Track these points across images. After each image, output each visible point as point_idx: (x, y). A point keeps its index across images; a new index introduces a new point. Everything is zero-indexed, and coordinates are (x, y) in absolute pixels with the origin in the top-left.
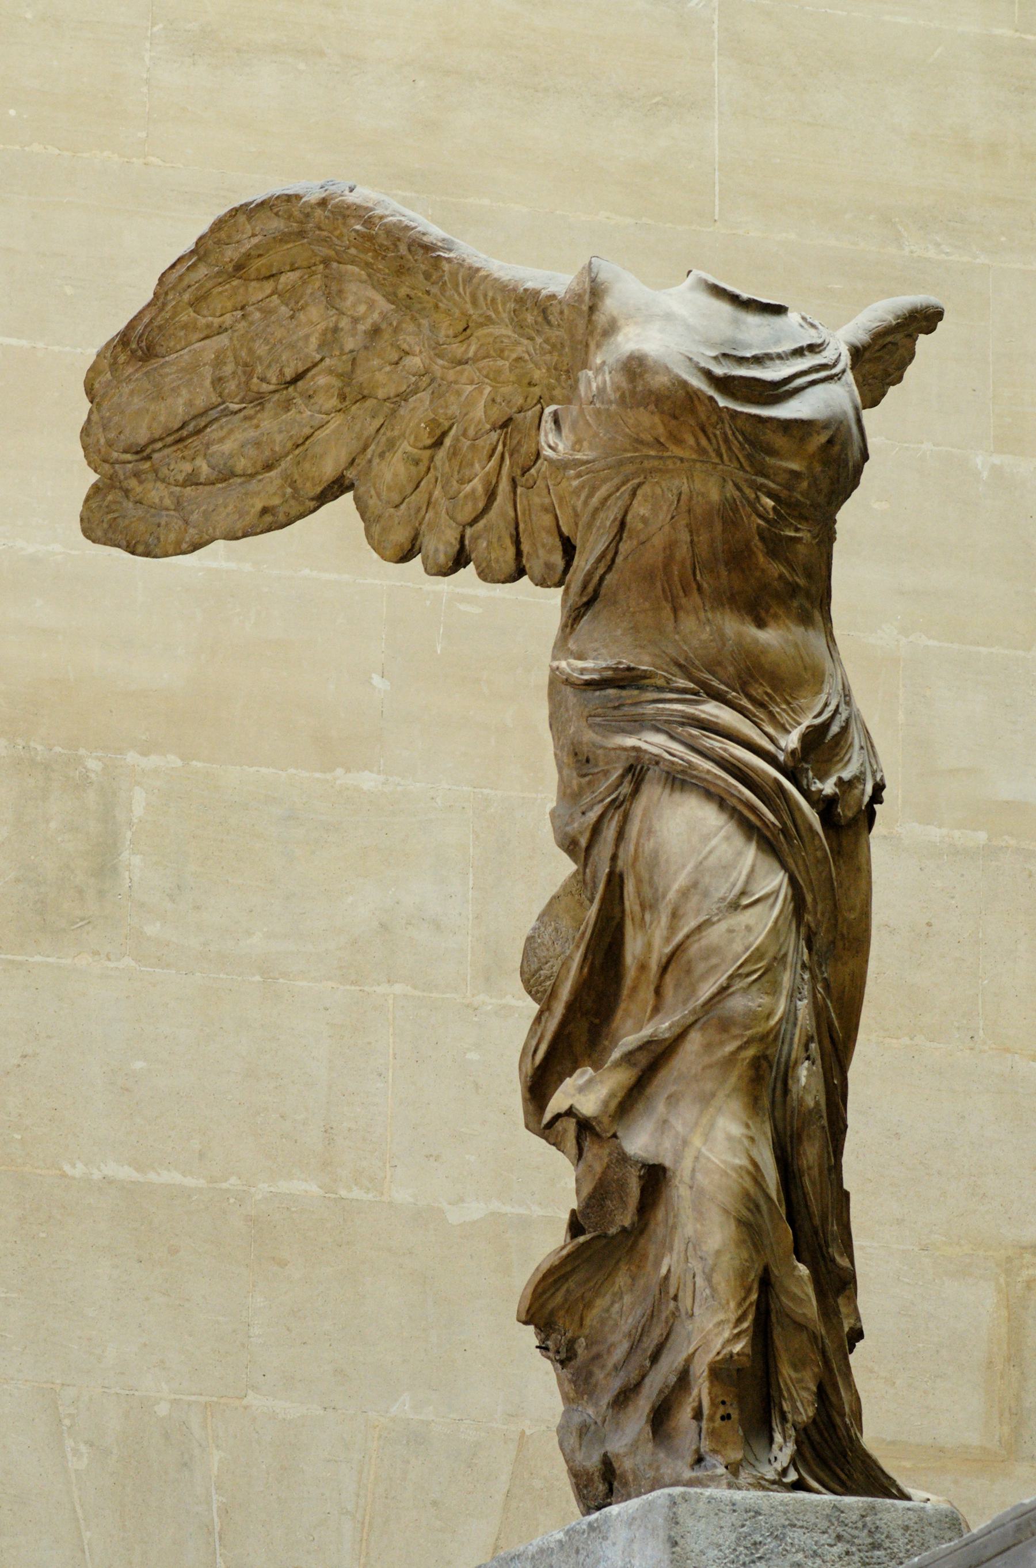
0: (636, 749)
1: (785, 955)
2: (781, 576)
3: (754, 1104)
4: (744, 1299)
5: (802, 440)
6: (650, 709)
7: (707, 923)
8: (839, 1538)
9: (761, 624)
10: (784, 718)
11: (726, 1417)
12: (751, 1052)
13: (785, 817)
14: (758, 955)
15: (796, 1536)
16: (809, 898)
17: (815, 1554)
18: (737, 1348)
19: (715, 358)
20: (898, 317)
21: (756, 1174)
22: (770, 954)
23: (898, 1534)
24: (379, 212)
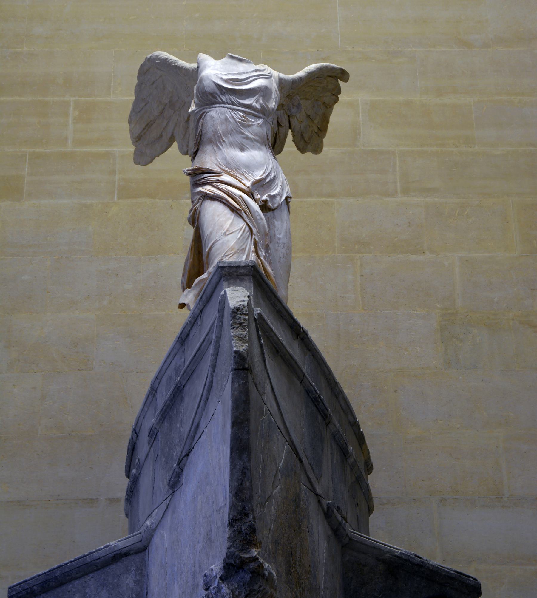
0: (201, 192)
6: (206, 180)
7: (216, 241)
10: (250, 178)
14: (232, 248)
16: (255, 231)
22: (236, 248)
24: (161, 56)
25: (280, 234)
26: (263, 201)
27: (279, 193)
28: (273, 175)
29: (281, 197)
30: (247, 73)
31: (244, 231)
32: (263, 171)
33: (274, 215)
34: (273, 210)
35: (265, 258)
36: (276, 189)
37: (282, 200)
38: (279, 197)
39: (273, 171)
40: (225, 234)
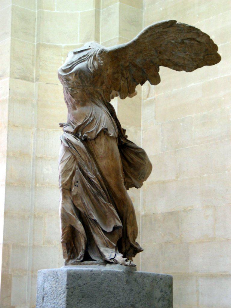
1: (72, 169)
2: (76, 100)
3: (64, 197)
4: (63, 232)
5: (72, 76)
8: (54, 277)
9: (76, 109)
11: (65, 252)
12: (61, 189)
13: (70, 144)
14: (62, 171)
15: (49, 278)
16: (77, 157)
17: (51, 281)
18: (62, 240)
19: (66, 66)
20: (145, 31)
21: (63, 209)
22: (64, 170)
23: (60, 276)
25: (100, 153)
26: (84, 137)
27: (95, 129)
28: (92, 119)
29: (97, 131)
30: (75, 61)
31: (70, 159)
32: (84, 120)
33: (96, 142)
34: (95, 139)
35: (86, 170)
36: (94, 127)
37: (98, 132)
38: (95, 131)
39: (92, 116)
40: (60, 164)
